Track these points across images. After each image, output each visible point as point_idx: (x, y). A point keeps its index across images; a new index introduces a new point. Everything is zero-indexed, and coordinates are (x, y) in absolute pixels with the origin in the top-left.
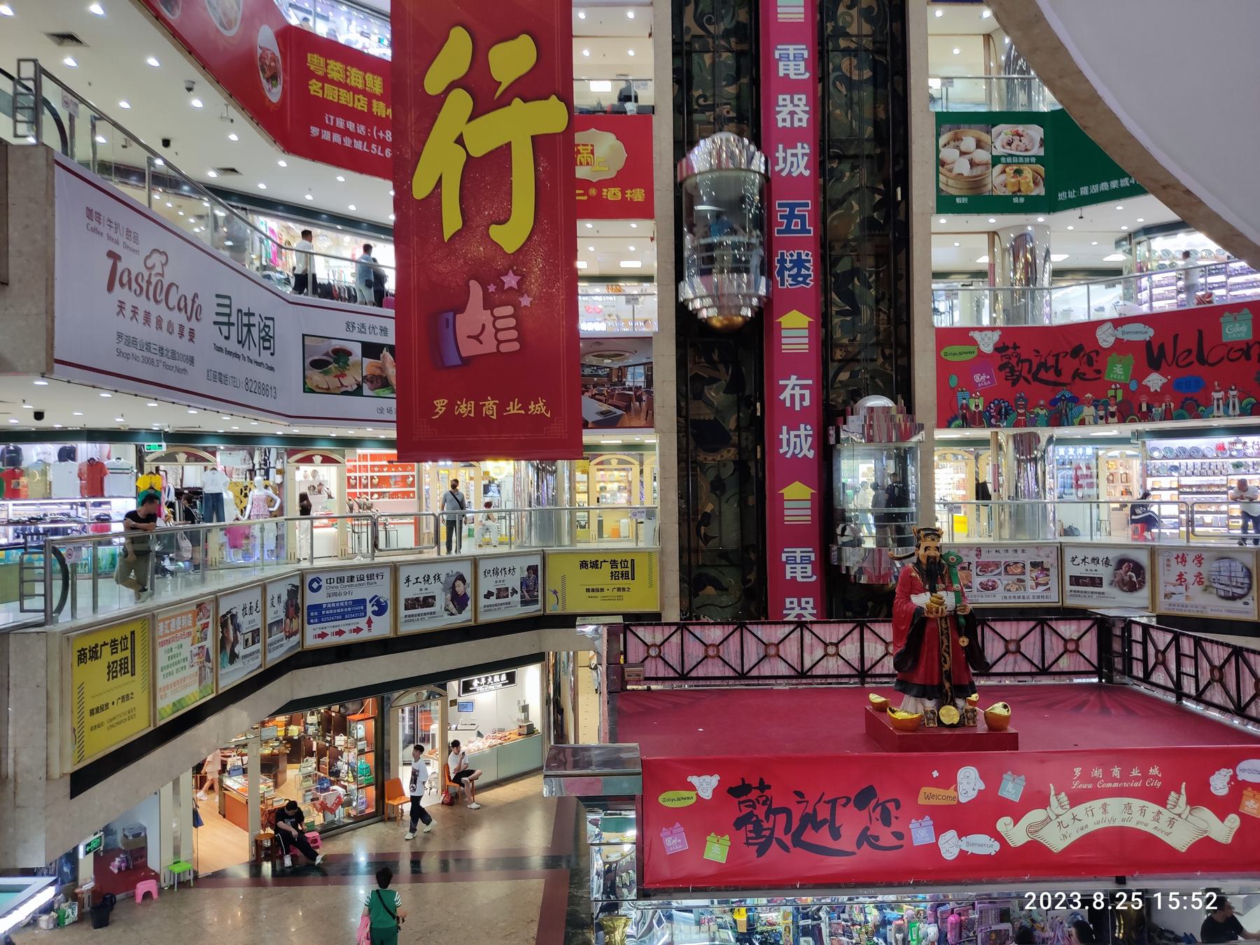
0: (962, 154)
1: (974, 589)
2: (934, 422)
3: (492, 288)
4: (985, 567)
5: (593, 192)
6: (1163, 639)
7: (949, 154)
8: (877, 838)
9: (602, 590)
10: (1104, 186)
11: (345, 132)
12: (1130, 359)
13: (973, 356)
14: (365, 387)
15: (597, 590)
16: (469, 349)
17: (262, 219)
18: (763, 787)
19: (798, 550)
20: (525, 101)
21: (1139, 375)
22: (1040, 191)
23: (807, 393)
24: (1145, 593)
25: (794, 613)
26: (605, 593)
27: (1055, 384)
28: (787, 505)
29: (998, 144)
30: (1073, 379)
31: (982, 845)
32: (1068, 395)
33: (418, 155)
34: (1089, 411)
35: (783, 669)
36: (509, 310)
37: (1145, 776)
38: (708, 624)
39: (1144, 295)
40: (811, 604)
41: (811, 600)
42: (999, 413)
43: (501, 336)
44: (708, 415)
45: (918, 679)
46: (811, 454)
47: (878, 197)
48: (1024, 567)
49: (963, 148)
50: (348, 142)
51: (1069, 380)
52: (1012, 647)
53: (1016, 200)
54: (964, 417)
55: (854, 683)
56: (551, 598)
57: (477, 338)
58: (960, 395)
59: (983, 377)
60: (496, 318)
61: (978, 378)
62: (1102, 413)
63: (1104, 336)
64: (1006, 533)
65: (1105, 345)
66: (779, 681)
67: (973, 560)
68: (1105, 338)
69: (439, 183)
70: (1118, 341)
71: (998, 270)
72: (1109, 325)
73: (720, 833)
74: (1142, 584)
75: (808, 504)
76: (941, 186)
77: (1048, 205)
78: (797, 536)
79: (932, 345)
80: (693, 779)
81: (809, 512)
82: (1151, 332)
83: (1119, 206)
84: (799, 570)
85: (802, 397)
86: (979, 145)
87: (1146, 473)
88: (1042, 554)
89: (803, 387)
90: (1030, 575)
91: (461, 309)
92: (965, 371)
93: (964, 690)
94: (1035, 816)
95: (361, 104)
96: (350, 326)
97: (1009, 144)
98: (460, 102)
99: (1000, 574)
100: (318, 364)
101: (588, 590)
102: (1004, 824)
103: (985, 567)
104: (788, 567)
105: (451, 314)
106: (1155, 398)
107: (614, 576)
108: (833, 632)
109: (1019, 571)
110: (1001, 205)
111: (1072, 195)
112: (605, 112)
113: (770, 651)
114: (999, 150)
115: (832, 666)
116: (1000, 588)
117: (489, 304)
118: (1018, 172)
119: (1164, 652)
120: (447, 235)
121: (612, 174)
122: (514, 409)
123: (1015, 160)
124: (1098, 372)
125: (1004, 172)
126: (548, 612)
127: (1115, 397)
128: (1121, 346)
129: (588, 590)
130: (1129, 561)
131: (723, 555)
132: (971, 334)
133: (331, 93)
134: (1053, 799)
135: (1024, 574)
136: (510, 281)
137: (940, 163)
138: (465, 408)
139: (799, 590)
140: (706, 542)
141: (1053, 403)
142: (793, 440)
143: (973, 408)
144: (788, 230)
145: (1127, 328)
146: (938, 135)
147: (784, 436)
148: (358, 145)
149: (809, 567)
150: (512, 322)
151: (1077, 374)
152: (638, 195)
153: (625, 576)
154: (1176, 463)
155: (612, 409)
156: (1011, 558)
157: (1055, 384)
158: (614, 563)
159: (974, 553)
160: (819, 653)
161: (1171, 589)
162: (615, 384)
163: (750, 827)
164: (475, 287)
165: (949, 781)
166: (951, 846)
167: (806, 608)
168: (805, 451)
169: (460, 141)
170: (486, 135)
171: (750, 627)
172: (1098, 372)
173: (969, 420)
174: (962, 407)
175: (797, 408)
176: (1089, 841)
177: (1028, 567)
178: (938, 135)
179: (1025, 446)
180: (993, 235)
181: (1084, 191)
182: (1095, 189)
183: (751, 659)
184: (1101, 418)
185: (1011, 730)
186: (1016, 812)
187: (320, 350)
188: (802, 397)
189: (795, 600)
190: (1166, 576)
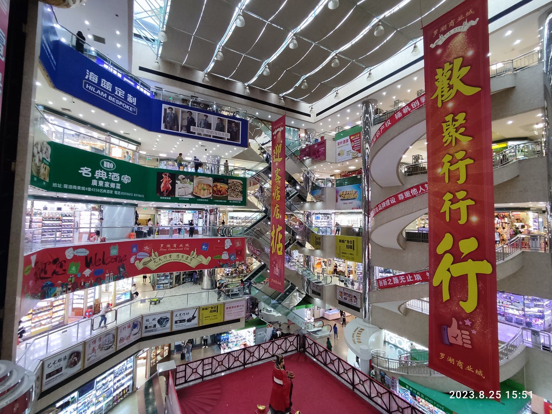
10: (75, 187)
12: (79, 264)
21: (82, 270)
30: (53, 274)
32: (49, 283)
34: (59, 289)
51: (50, 276)
62: (64, 289)
63: (69, 254)
65: (69, 258)
68: (69, 255)
70: (75, 256)
72: (71, 249)
74: (79, 360)
82: (88, 252)
106: (87, 279)
111: (60, 186)
124: (65, 270)
127: (71, 281)
151: (54, 272)
172: (65, 270)
181: (66, 186)
182: (71, 187)
184: (64, 291)
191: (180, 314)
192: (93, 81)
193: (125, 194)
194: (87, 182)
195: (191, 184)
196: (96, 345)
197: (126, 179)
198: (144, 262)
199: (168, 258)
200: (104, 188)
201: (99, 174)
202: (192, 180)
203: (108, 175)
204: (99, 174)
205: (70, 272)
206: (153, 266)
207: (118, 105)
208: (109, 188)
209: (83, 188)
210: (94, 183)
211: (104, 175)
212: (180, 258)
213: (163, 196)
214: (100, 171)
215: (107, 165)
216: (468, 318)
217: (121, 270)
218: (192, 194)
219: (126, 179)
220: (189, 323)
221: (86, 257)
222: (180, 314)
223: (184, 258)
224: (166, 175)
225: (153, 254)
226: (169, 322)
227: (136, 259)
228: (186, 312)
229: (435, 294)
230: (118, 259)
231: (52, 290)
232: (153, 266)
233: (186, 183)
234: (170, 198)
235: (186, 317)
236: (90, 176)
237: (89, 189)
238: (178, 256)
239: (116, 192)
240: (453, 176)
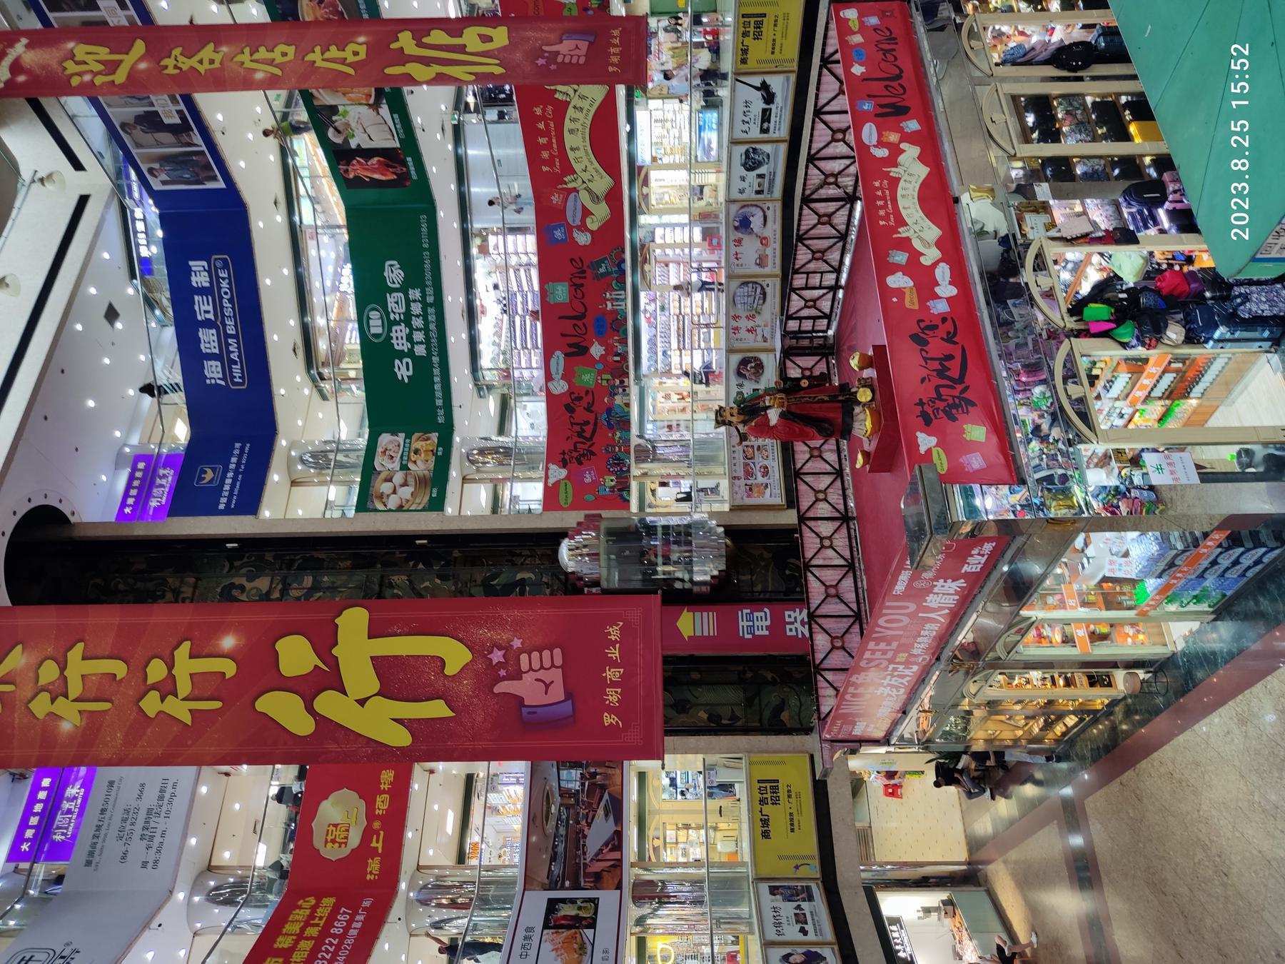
0: (394, 492)
3: (503, 673)
4: (749, 474)
5: (377, 825)
6: (796, 303)
7: (393, 502)
8: (949, 333)
9: (791, 814)
10: (437, 387)
13: (569, 485)
15: (792, 820)
16: (557, 693)
18: (921, 403)
19: (741, 623)
20: (336, 644)
21: (591, 362)
24: (763, 357)
25: (800, 628)
26: (794, 811)
27: (595, 424)
28: (699, 633)
29: (390, 466)
31: (943, 273)
33: (395, 635)
34: (618, 400)
35: (848, 583)
36: (524, 658)
37: (881, 188)
38: (812, 646)
39: (526, 374)
40: (791, 613)
41: (787, 613)
43: (547, 664)
45: (837, 417)
47: (421, 566)
52: (816, 453)
54: (620, 490)
55: (854, 525)
56: (803, 872)
57: (547, 686)
58: (601, 493)
60: (531, 669)
61: (588, 480)
64: (720, 470)
65: (566, 387)
66: (859, 585)
67: (743, 482)
68: (560, 387)
69: (399, 721)
71: (493, 476)
72: (550, 385)
73: (963, 431)
74: (756, 359)
75: (698, 615)
77: (446, 433)
78: (727, 625)
79: (558, 514)
80: (922, 450)
81: (705, 614)
83: (455, 380)
84: (759, 623)
86: (389, 480)
87: (668, 373)
91: (520, 700)
92: (580, 488)
93: (844, 388)
94: (917, 244)
98: (328, 703)
101: (792, 830)
102: (926, 261)
103: (749, 474)
104: (757, 633)
105: (525, 710)
106: (610, 350)
107: (776, 802)
108: (816, 591)
110: (443, 464)
111: (441, 412)
112: (297, 813)
113: (832, 593)
114: (396, 465)
115: (841, 541)
116: (766, 463)
117: (517, 675)
118: (417, 452)
119: (806, 301)
120: (449, 713)
121: (362, 805)
122: (614, 653)
124: (587, 392)
126: (818, 876)
128: (568, 376)
129: (792, 830)
130: (738, 369)
131: (749, 702)
134: (904, 235)
136: (497, 656)
137: (400, 508)
138: (613, 697)
139: (778, 624)
140: (738, 719)
141: (611, 427)
145: (553, 370)
146: (376, 510)
149: (756, 614)
150: (535, 655)
151: (588, 409)
153: (775, 790)
154: (660, 354)
155: (602, 804)
157: (595, 424)
158: (763, 802)
159: (737, 482)
160: (830, 553)
161: (759, 338)
162: (577, 801)
163: (954, 411)
164: (501, 688)
165: (899, 292)
166: (946, 289)
167: (795, 619)
169: (362, 702)
170: (359, 674)
171: (799, 466)
172: (587, 392)
173: (625, 487)
176: (929, 214)
178: (376, 510)
179: (647, 454)
180: (465, 480)
181: (439, 402)
182: (439, 394)
183: (840, 609)
185: (871, 353)
186: (915, 255)
189: (788, 627)
190: (750, 341)
191: (744, 122)
192: (215, 338)
193: (428, 275)
194: (422, 365)
195: (346, 112)
196: (744, 324)
197: (394, 273)
198: (593, 201)
199: (580, 153)
200: (426, 329)
201: (400, 341)
202: (333, 110)
203: (397, 323)
204: (401, 344)
205: (592, 384)
206: (602, 183)
207: (233, 308)
208: (425, 316)
209: (436, 371)
210: (420, 350)
211: (399, 332)
212: (578, 125)
213: (408, 172)
214: (394, 341)
215: (376, 326)
216: (485, 656)
217: (602, 270)
218: (375, 106)
219: (394, 273)
220: (779, 99)
221: (566, 355)
222: (744, 122)
223: (578, 115)
224: (346, 171)
225: (571, 186)
226: (758, 146)
227: (583, 227)
228: (740, 108)
229: (433, 743)
230: (578, 281)
231: (617, 410)
232: (602, 183)
233: (348, 125)
234: (409, 159)
235: (758, 105)
236: (409, 360)
237: (436, 359)
238: (571, 131)
239: (430, 299)
240: (100, 689)
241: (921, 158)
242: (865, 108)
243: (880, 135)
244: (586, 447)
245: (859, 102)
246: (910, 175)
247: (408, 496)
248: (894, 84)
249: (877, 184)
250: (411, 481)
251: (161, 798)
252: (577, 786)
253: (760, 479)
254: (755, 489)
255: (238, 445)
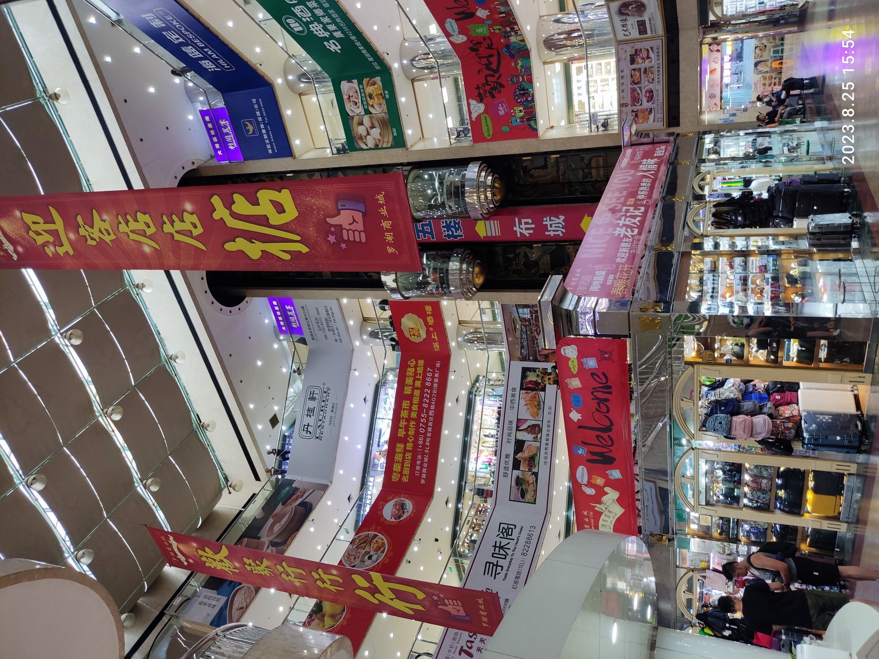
0: (368, 134)
1: (652, 106)
2: (534, 140)
4: (635, 100)
7: (371, 143)
11: (421, 465)
14: (534, 470)
17: (470, 469)
22: (378, 79)
23: (523, 221)
29: (357, 111)
37: (588, 516)
42: (523, 95)
44: (547, 258)
46: (562, 217)
48: (634, 70)
49: (364, 133)
50: (425, 465)
53: (387, 96)
54: (529, 120)
58: (514, 124)
59: (501, 108)
61: (502, 113)
67: (630, 108)
76: (389, 146)
79: (484, 145)
85: (526, 223)
86: (361, 123)
88: (623, 56)
89: (520, 223)
90: (641, 64)
95: (409, 455)
96: (505, 475)
97: (356, 103)
99: (640, 88)
100: (523, 496)
109: (637, 73)
114: (361, 110)
116: (651, 86)
118: (371, 96)
123: (364, 99)
125: (372, 106)
132: (474, 119)
133: (406, 471)
135: (640, 69)
137: (377, 147)
141: (513, 57)
142: (553, 228)
143: (522, 114)
144: (431, 233)
147: (552, 233)
148: (426, 460)
152: (428, 309)
156: (628, 80)
159: (624, 109)
168: (560, 221)
174: (522, 122)
175: (533, 226)
177: (635, 66)
182: (367, 55)
187: (516, 493)
188: (526, 223)
241: (619, 501)
242: (580, 452)
243: (590, 478)
244: (494, 79)
245: (575, 447)
246: (610, 512)
247: (378, 137)
248: (605, 435)
249: (585, 513)
250: (376, 124)
251: (328, 314)
252: (529, 316)
253: (646, 105)
254: (640, 115)
255: (254, 101)
